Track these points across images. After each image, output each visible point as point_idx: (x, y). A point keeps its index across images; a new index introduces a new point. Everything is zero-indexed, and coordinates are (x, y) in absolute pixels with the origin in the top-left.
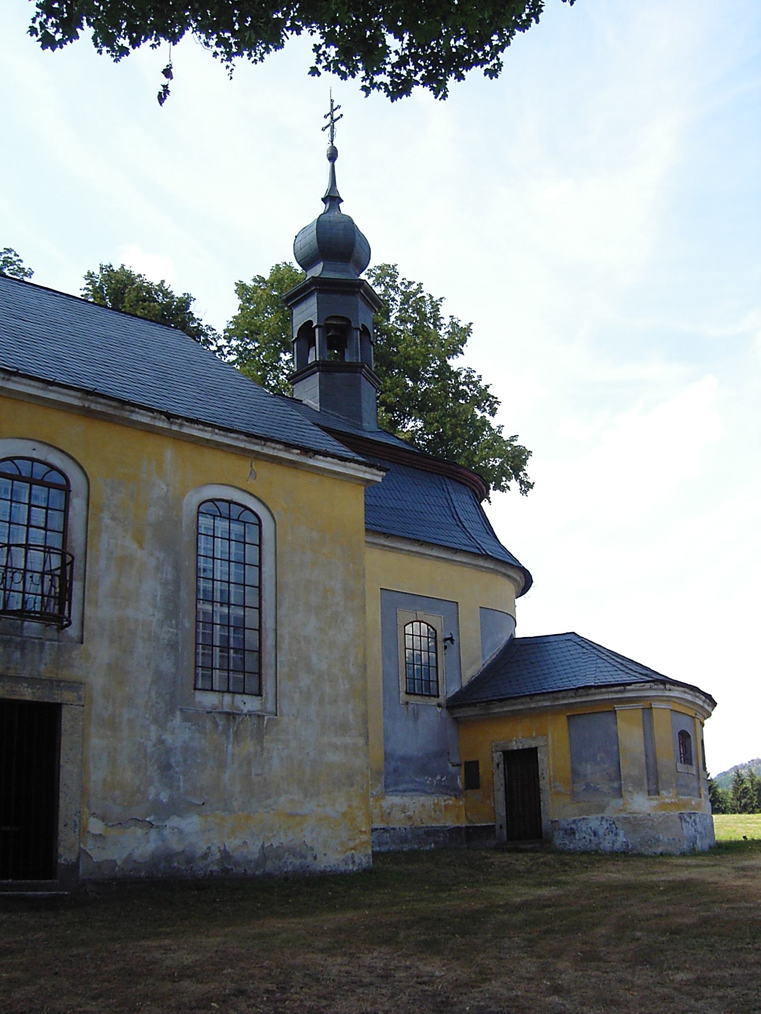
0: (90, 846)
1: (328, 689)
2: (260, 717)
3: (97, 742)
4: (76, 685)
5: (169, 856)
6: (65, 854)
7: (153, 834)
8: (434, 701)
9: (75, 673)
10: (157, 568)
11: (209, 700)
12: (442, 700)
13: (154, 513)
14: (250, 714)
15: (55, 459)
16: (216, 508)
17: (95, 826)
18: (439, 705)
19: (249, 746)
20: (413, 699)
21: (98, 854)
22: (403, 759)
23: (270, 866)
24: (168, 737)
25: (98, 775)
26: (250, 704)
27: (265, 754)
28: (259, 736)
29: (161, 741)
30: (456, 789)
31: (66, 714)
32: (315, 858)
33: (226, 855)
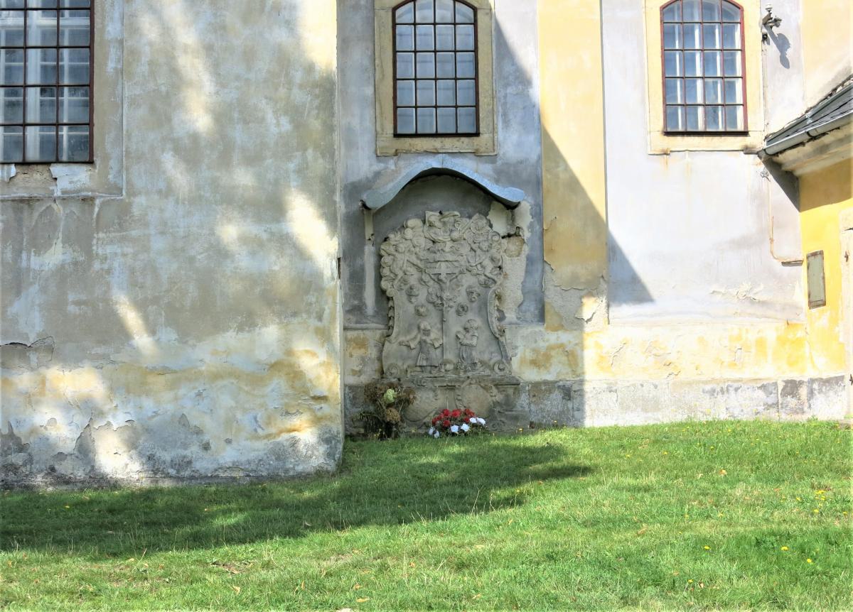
2: (87, 201)
8: (738, 142)
12: (757, 139)
14: (66, 199)
18: (748, 151)
19: (56, 255)
26: (71, 177)
27: (97, 266)
28: (81, 239)
30: (795, 307)
32: (206, 447)
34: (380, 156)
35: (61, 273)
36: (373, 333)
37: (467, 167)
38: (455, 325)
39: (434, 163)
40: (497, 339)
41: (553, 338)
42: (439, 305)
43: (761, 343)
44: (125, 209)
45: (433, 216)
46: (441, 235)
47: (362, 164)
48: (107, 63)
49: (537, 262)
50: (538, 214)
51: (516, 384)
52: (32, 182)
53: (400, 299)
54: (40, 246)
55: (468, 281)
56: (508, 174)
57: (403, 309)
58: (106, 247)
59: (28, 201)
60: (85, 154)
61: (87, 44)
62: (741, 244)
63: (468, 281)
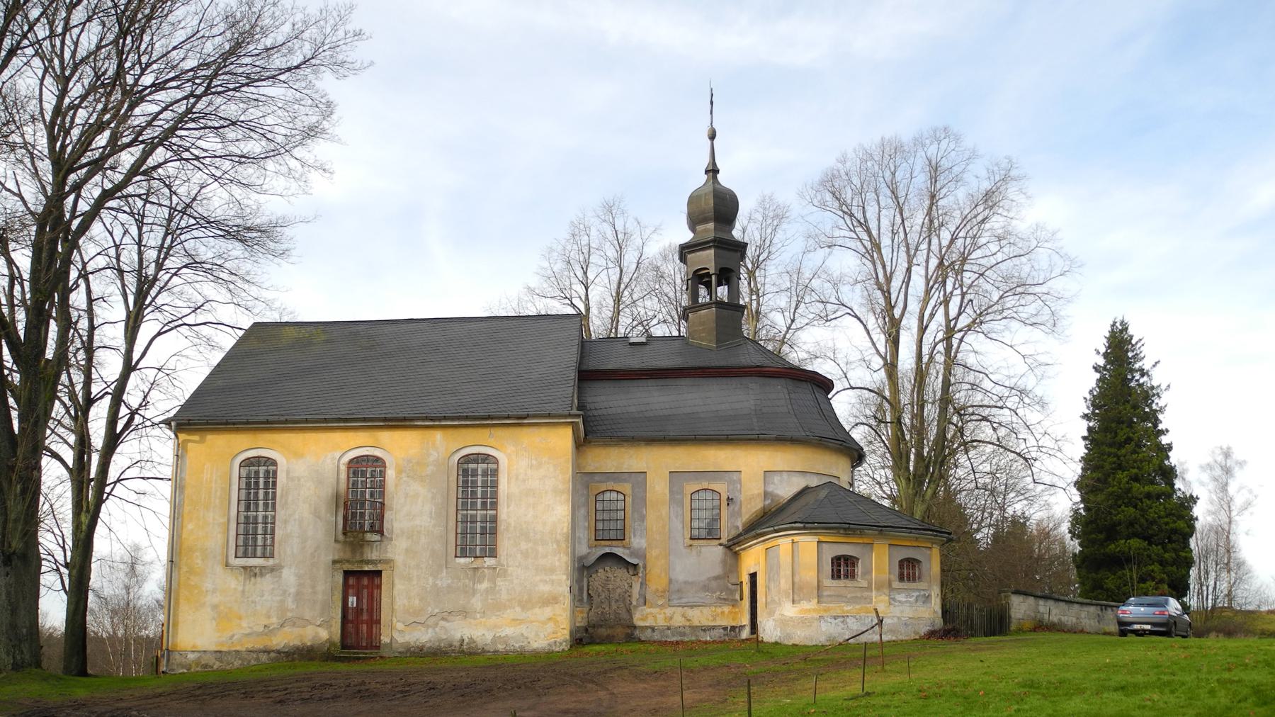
0: (396, 635)
1: (540, 549)
3: (400, 586)
4: (388, 562)
5: (440, 640)
6: (385, 639)
7: (430, 630)
9: (389, 556)
10: (433, 498)
11: (462, 560)
12: (724, 541)
13: (429, 470)
14: (488, 568)
15: (377, 453)
16: (467, 459)
17: (400, 626)
19: (485, 585)
20: (696, 542)
21: (400, 639)
22: (686, 583)
23: (500, 647)
24: (439, 583)
25: (400, 602)
26: (489, 561)
29: (435, 585)
31: (383, 574)
33: (472, 640)
34: (590, 547)
35: (487, 591)
36: (586, 609)
37: (619, 551)
38: (614, 607)
39: (607, 550)
40: (629, 611)
41: (649, 610)
42: (608, 598)
43: (723, 613)
44: (506, 571)
45: (607, 568)
46: (610, 575)
47: (583, 549)
48: (501, 527)
49: (643, 584)
50: (645, 567)
51: (635, 627)
52: (478, 563)
53: (595, 597)
54: (480, 582)
55: (619, 591)
56: (634, 553)
57: (596, 600)
58: (499, 582)
59: (477, 569)
60: (493, 554)
61: (494, 520)
62: (716, 578)
63: (619, 591)
